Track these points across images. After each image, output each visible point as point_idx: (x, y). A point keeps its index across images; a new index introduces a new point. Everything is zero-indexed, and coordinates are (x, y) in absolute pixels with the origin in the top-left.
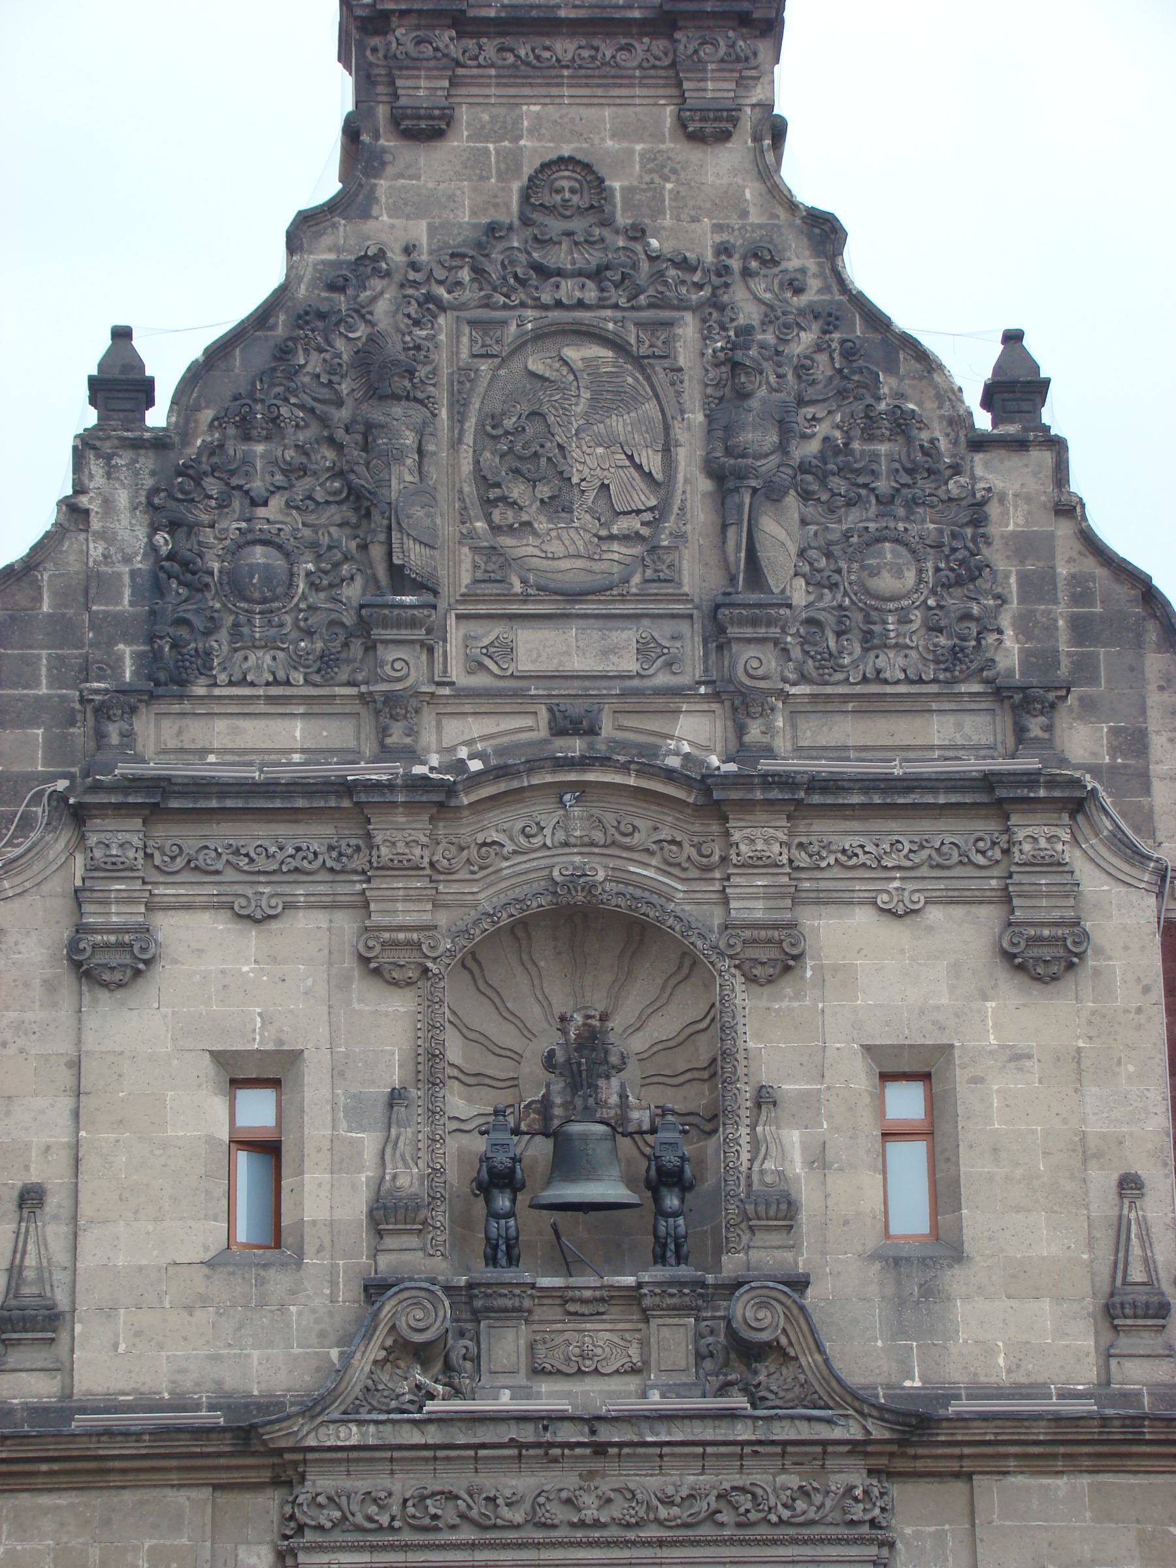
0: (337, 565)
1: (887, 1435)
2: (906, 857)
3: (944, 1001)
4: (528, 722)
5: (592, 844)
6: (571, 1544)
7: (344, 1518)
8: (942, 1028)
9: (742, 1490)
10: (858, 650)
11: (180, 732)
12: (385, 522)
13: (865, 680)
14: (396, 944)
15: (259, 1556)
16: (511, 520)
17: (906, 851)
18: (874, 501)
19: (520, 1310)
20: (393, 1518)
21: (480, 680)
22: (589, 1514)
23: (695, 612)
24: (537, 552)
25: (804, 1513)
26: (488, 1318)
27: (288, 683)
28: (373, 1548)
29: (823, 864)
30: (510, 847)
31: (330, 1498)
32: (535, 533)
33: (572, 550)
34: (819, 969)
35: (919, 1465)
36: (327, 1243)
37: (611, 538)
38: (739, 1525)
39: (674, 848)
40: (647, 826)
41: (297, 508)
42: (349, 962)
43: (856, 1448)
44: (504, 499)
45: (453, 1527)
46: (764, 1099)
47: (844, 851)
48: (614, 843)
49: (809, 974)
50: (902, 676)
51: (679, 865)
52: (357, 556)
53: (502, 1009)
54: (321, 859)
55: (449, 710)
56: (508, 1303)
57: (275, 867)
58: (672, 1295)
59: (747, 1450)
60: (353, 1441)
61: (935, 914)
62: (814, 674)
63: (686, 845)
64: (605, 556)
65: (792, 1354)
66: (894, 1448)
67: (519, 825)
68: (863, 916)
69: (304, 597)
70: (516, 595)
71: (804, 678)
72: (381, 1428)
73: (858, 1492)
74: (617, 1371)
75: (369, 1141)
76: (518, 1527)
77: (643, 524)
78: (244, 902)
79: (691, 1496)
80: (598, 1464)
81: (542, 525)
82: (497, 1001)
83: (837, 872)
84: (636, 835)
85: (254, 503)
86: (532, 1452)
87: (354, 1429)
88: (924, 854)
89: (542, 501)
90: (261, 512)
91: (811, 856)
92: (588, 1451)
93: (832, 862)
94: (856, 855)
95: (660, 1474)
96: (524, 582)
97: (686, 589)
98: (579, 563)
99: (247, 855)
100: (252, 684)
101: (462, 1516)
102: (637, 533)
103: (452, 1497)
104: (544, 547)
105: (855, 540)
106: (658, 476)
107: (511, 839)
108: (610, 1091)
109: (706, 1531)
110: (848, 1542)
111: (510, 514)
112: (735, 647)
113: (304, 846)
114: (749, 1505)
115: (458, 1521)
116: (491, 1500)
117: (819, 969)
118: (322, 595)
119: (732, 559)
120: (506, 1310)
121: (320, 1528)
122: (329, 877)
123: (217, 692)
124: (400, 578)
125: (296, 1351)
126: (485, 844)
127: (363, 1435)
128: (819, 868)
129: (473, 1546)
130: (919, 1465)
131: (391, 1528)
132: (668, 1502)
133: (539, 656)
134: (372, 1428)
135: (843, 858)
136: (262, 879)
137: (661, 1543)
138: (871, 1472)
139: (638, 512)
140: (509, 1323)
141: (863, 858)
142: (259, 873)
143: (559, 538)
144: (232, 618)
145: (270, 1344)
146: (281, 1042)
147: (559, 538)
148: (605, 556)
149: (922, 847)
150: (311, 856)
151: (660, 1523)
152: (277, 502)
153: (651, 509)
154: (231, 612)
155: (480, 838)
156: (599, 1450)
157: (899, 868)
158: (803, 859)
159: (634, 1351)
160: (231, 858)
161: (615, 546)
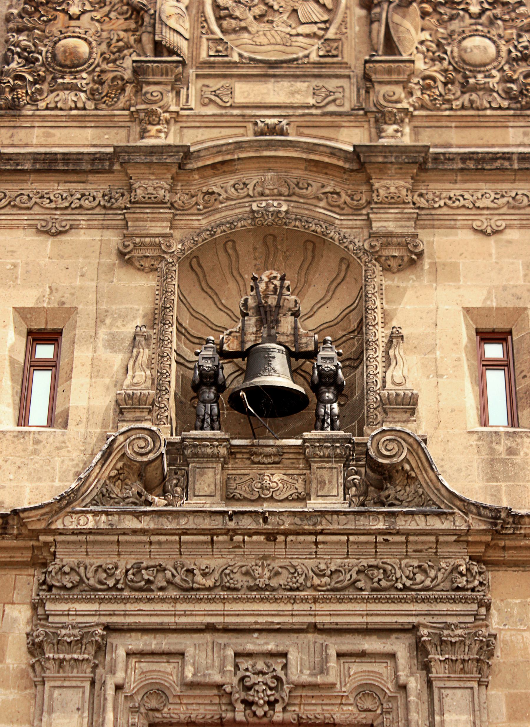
0: (120, 50)
1: (483, 527)
2: (492, 201)
3: (521, 282)
4: (241, 131)
5: (281, 195)
6: (248, 600)
7: (81, 581)
8: (519, 298)
9: (377, 567)
10: (459, 93)
11: (12, 136)
12: (152, 21)
13: (463, 108)
14: (143, 244)
15: (20, 612)
16: (234, 26)
17: (492, 198)
18: (467, 16)
19: (217, 456)
20: (118, 581)
21: (211, 110)
22: (261, 583)
23: (352, 74)
24: (251, 42)
25: (423, 582)
26: (194, 462)
27: (84, 109)
28: (101, 601)
29: (436, 205)
30: (224, 195)
31: (72, 569)
32: (249, 32)
33: (273, 41)
34: (434, 264)
35: (508, 555)
36: (84, 420)
37: (298, 35)
38: (374, 590)
39: (335, 196)
40: (317, 183)
41: (98, 21)
42: (113, 259)
43: (461, 537)
44: (231, 16)
45: (161, 589)
46: (395, 338)
47: (450, 198)
48: (294, 194)
49: (426, 267)
50: (488, 106)
51: (339, 206)
52: (135, 46)
53: (218, 303)
54: (97, 200)
55: (189, 124)
56: (209, 451)
57: (67, 204)
58: (327, 447)
59: (380, 539)
60: (90, 525)
61: (512, 235)
62: (429, 103)
63: (343, 195)
64: (294, 44)
65: (413, 475)
66: (488, 538)
67: (232, 182)
68: (465, 236)
69: (98, 65)
70: (235, 63)
71: (423, 107)
72: (110, 518)
73: (463, 568)
74: (287, 499)
75: (117, 359)
76: (210, 589)
77: (319, 29)
78: (44, 224)
79: (337, 571)
80: (269, 549)
81: (254, 27)
82: (215, 297)
83: (445, 210)
84: (310, 188)
85: (71, 18)
86: (221, 538)
87: (90, 516)
88: (505, 200)
89: (255, 18)
90: (73, 23)
91: (428, 201)
92: (262, 538)
93: (442, 205)
94: (459, 200)
95: (316, 558)
96: (240, 55)
97: (345, 60)
98: (277, 47)
99: (49, 198)
100: (61, 109)
101: (169, 582)
102: (315, 34)
103: (161, 569)
104: (255, 39)
105: (456, 36)
106: (330, 6)
107: (226, 192)
108: (286, 324)
109: (351, 593)
110: (454, 601)
111: (233, 21)
112: (377, 87)
113: (87, 193)
114: (381, 576)
115: (164, 584)
116: (190, 571)
117: (434, 264)
118: (111, 65)
119: (375, 41)
120: (208, 456)
121: (64, 588)
122: (103, 212)
123: (38, 113)
124: (159, 48)
125: (57, 483)
126: (208, 193)
127: (97, 522)
128: (434, 208)
129: (175, 600)
130: (508, 555)
131: (115, 588)
132: (321, 574)
133: (249, 94)
134: (104, 518)
135: (449, 202)
136: (58, 212)
137: (315, 600)
138: (471, 558)
139: (316, 23)
140: (210, 465)
141: (462, 202)
142: (56, 209)
143: (265, 35)
144: (51, 76)
145: (39, 479)
146: (63, 303)
147: (265, 35)
148: (294, 44)
149: (503, 196)
150: (91, 199)
151: (314, 587)
152: (86, 18)
153: (325, 22)
154: (51, 73)
155: (205, 189)
156: (271, 536)
157: (488, 208)
158: (422, 202)
159: (300, 486)
160: (38, 200)
161: (300, 39)
